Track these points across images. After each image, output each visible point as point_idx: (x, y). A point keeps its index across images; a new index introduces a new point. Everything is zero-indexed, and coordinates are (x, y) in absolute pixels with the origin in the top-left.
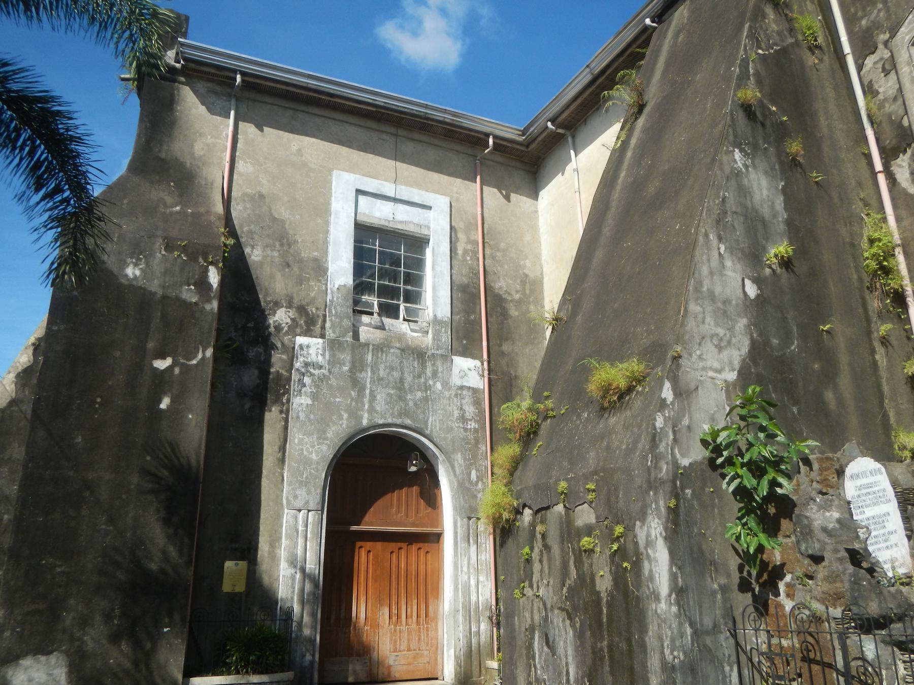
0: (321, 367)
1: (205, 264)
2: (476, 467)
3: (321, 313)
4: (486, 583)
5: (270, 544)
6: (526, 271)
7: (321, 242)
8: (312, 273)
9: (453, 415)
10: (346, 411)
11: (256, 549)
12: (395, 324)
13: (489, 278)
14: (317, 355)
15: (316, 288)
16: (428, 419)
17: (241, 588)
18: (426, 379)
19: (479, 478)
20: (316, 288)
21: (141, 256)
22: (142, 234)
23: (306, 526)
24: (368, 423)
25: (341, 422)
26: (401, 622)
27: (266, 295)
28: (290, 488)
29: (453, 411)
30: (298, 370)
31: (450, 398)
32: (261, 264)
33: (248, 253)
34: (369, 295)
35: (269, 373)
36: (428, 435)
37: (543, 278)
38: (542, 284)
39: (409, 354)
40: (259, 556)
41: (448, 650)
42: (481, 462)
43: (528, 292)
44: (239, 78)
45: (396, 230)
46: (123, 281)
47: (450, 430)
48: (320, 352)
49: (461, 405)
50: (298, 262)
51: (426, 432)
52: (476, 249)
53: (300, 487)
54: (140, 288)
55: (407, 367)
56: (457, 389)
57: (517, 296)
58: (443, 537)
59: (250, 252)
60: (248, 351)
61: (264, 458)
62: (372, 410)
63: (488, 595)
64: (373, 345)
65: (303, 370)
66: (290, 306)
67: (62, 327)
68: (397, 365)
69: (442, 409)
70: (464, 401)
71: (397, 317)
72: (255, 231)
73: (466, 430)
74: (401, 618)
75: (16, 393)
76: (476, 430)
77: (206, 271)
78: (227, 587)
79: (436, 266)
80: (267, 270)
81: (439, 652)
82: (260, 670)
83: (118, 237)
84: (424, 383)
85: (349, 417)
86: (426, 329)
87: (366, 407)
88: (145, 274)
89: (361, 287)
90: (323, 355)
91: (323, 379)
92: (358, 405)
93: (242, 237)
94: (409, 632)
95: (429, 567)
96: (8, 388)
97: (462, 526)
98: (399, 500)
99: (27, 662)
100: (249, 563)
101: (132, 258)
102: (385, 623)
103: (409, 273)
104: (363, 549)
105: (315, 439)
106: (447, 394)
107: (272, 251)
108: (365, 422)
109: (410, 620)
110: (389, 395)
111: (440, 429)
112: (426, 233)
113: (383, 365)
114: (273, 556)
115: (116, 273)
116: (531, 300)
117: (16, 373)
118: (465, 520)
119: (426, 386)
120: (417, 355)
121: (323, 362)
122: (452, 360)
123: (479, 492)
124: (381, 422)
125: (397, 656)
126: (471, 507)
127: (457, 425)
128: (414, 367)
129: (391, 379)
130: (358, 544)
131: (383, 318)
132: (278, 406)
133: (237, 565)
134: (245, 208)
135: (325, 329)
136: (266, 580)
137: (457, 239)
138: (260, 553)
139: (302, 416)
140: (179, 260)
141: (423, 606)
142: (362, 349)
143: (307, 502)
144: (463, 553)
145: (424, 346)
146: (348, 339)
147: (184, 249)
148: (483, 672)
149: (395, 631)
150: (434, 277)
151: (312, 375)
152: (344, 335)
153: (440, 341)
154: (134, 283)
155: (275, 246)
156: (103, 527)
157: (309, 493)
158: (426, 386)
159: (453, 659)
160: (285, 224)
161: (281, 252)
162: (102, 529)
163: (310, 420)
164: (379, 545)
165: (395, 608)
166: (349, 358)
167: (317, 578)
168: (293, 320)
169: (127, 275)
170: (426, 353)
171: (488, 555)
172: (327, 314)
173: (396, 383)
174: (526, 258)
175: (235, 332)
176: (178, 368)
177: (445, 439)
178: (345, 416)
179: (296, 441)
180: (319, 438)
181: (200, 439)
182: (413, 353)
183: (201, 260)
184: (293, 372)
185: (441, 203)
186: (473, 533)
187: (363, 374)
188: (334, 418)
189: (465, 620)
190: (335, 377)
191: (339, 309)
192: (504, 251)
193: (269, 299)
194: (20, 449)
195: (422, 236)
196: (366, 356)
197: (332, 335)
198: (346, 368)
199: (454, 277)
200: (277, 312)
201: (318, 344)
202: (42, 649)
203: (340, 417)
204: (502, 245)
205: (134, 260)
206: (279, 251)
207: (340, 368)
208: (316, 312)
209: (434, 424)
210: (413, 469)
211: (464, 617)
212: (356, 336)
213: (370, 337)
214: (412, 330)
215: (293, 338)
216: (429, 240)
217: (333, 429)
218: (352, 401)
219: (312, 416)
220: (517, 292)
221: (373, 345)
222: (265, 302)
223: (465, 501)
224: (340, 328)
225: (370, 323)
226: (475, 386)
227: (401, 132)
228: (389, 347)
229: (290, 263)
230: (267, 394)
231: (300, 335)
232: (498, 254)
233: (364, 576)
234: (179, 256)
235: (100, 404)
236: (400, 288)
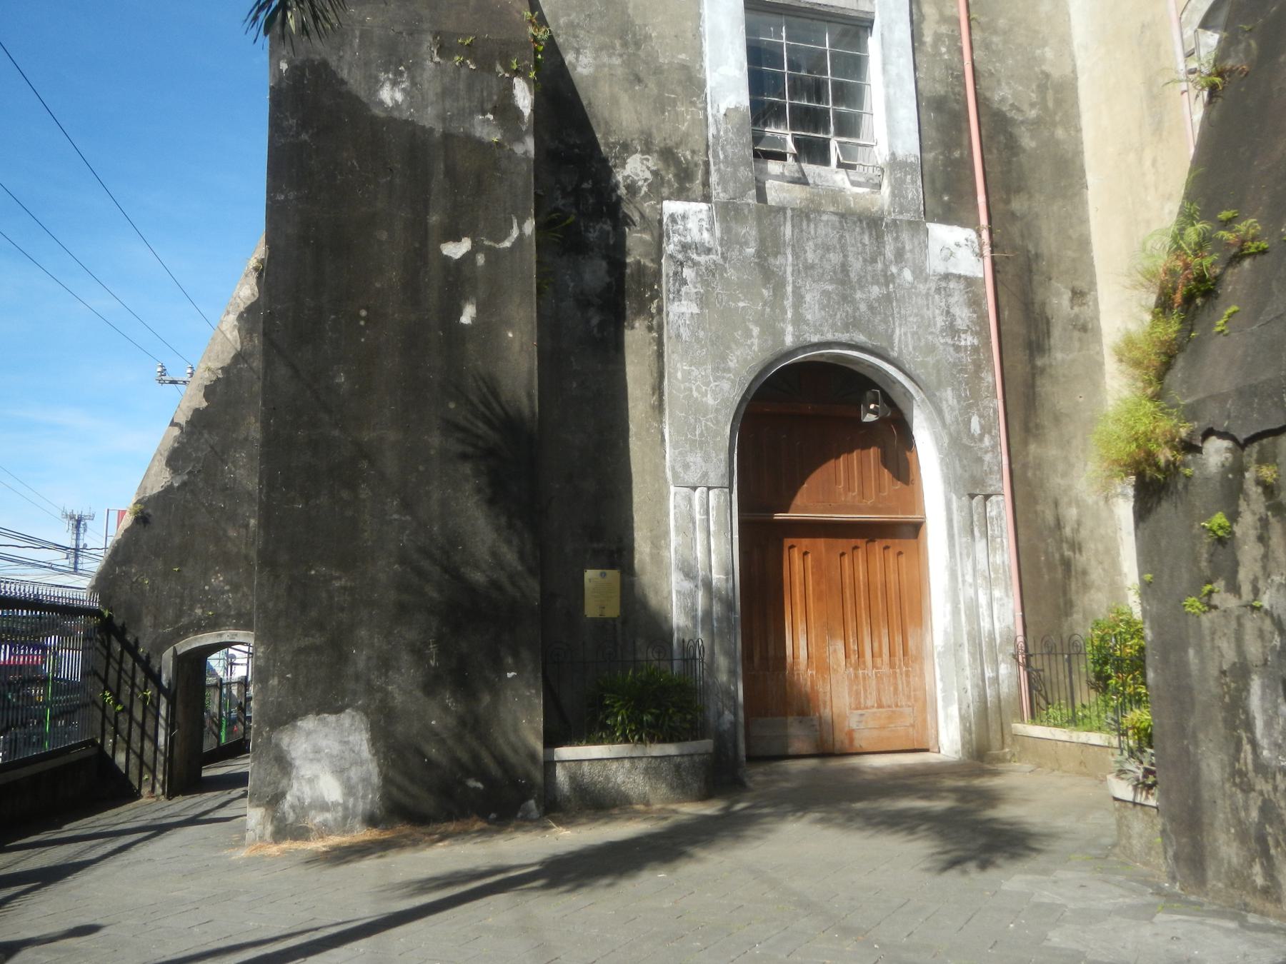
1: (507, 75)
2: (978, 410)
3: (700, 159)
4: (1006, 600)
5: (652, 543)
6: (1045, 68)
7: (689, 35)
8: (679, 89)
9: (935, 325)
10: (756, 323)
11: (630, 550)
12: (823, 174)
13: (984, 83)
14: (700, 231)
15: (688, 117)
16: (893, 332)
17: (613, 611)
18: (884, 264)
19: (986, 429)
20: (688, 117)
21: (402, 68)
22: (398, 28)
23: (707, 513)
24: (793, 342)
25: (749, 342)
26: (864, 663)
27: (607, 133)
28: (677, 451)
29: (934, 318)
30: (671, 256)
31: (927, 295)
32: (595, 79)
33: (570, 62)
34: (777, 126)
35: (623, 265)
36: (894, 359)
37: (1076, 78)
38: (1074, 89)
39: (855, 223)
40: (636, 561)
41: (946, 707)
42: (986, 402)
43: (1051, 104)
45: (815, 7)
46: (377, 112)
47: (931, 349)
48: (705, 226)
49: (948, 307)
50: (655, 73)
51: (891, 353)
52: (956, 33)
53: (691, 451)
54: (406, 121)
55: (853, 246)
56: (939, 279)
57: (1033, 113)
58: (926, 529)
59: (574, 61)
60: (587, 230)
61: (631, 404)
62: (798, 320)
63: (1009, 620)
64: (793, 209)
65: (680, 257)
66: (647, 150)
67: (292, 195)
68: (835, 241)
69: (916, 315)
70: (952, 300)
71: (826, 162)
72: (578, 24)
73: (957, 348)
74: (864, 657)
75: (242, 343)
76: (975, 349)
77: (510, 87)
79: (889, 67)
80: (605, 89)
81: (929, 709)
82: (661, 737)
83: (361, 37)
84: (882, 271)
85: (762, 333)
86: (876, 181)
87: (789, 315)
88: (412, 97)
89: (762, 112)
90: (711, 230)
92: (775, 312)
93: (558, 35)
94: (879, 678)
95: (904, 577)
96: (229, 336)
97: (960, 509)
98: (848, 469)
99: (308, 723)
100: (622, 573)
101: (387, 72)
102: (839, 665)
103: (842, 83)
104: (796, 549)
105: (709, 371)
106: (922, 288)
107: (610, 56)
108: (789, 340)
109: (878, 661)
110: (825, 293)
111: (914, 348)
112: (867, 9)
113: (811, 243)
114: (658, 559)
115: (365, 100)
116: (1057, 118)
117: (238, 313)
118: (965, 499)
119: (885, 276)
120: (868, 224)
121: (712, 243)
122: (927, 231)
123: (986, 452)
124: (815, 339)
125: (862, 715)
126: (973, 478)
127: (942, 341)
128: (864, 245)
129: (828, 267)
130: (788, 542)
131: (803, 165)
132: (645, 319)
133: (603, 575)
135: (709, 187)
136: (653, 601)
137: (922, 17)
138: (637, 557)
139: (685, 333)
140: (463, 71)
141: (898, 639)
142: (775, 217)
143: (705, 475)
144: (965, 552)
145: (876, 209)
146: (750, 201)
147: (469, 51)
148: (1008, 740)
149: (856, 676)
150: (887, 86)
151: (695, 264)
152: (743, 194)
153: (904, 198)
154: (396, 114)
155: (614, 48)
156: (396, 516)
157: (706, 459)
158: (885, 276)
159: (957, 720)
160: (627, 8)
161: (625, 57)
162: (395, 520)
163: (698, 340)
164: (821, 543)
165: (854, 641)
166: (754, 233)
167: (731, 594)
168: (655, 173)
169: (382, 103)
170: (882, 219)
171: (1006, 556)
172: (711, 160)
173: (835, 272)
174: (1045, 43)
175: (562, 198)
176: (483, 255)
177: (924, 364)
178: (756, 331)
179: (679, 375)
180: (716, 369)
181: (530, 372)
182: (861, 221)
183: (499, 68)
184: (663, 261)
186: (978, 521)
187: (780, 260)
188: (738, 334)
189: (975, 660)
190: (735, 268)
191: (729, 149)
192: (1005, 33)
193: (612, 140)
195: (861, 15)
196: (782, 228)
197: (721, 195)
198: (750, 251)
199: (921, 84)
200: (628, 161)
201: (701, 211)
202: (329, 705)
203: (748, 334)
204: (1002, 23)
205: (391, 76)
206: (621, 56)
207: (740, 252)
208: (692, 157)
209: (903, 339)
210: (870, 418)
211: (973, 655)
212: (761, 195)
213: (784, 198)
214: (854, 183)
215: (658, 203)
216: (872, 22)
217: (738, 353)
218: (764, 305)
219: (701, 334)
220: (1032, 105)
221: (793, 209)
222: (607, 144)
223: (963, 467)
224: (735, 182)
225: (783, 174)
226: (969, 274)
228: (819, 212)
229: (642, 75)
230: (623, 299)
231: (669, 199)
232: (995, 39)
233: (800, 592)
234: (463, 63)
235: (367, 319)
236: (827, 111)
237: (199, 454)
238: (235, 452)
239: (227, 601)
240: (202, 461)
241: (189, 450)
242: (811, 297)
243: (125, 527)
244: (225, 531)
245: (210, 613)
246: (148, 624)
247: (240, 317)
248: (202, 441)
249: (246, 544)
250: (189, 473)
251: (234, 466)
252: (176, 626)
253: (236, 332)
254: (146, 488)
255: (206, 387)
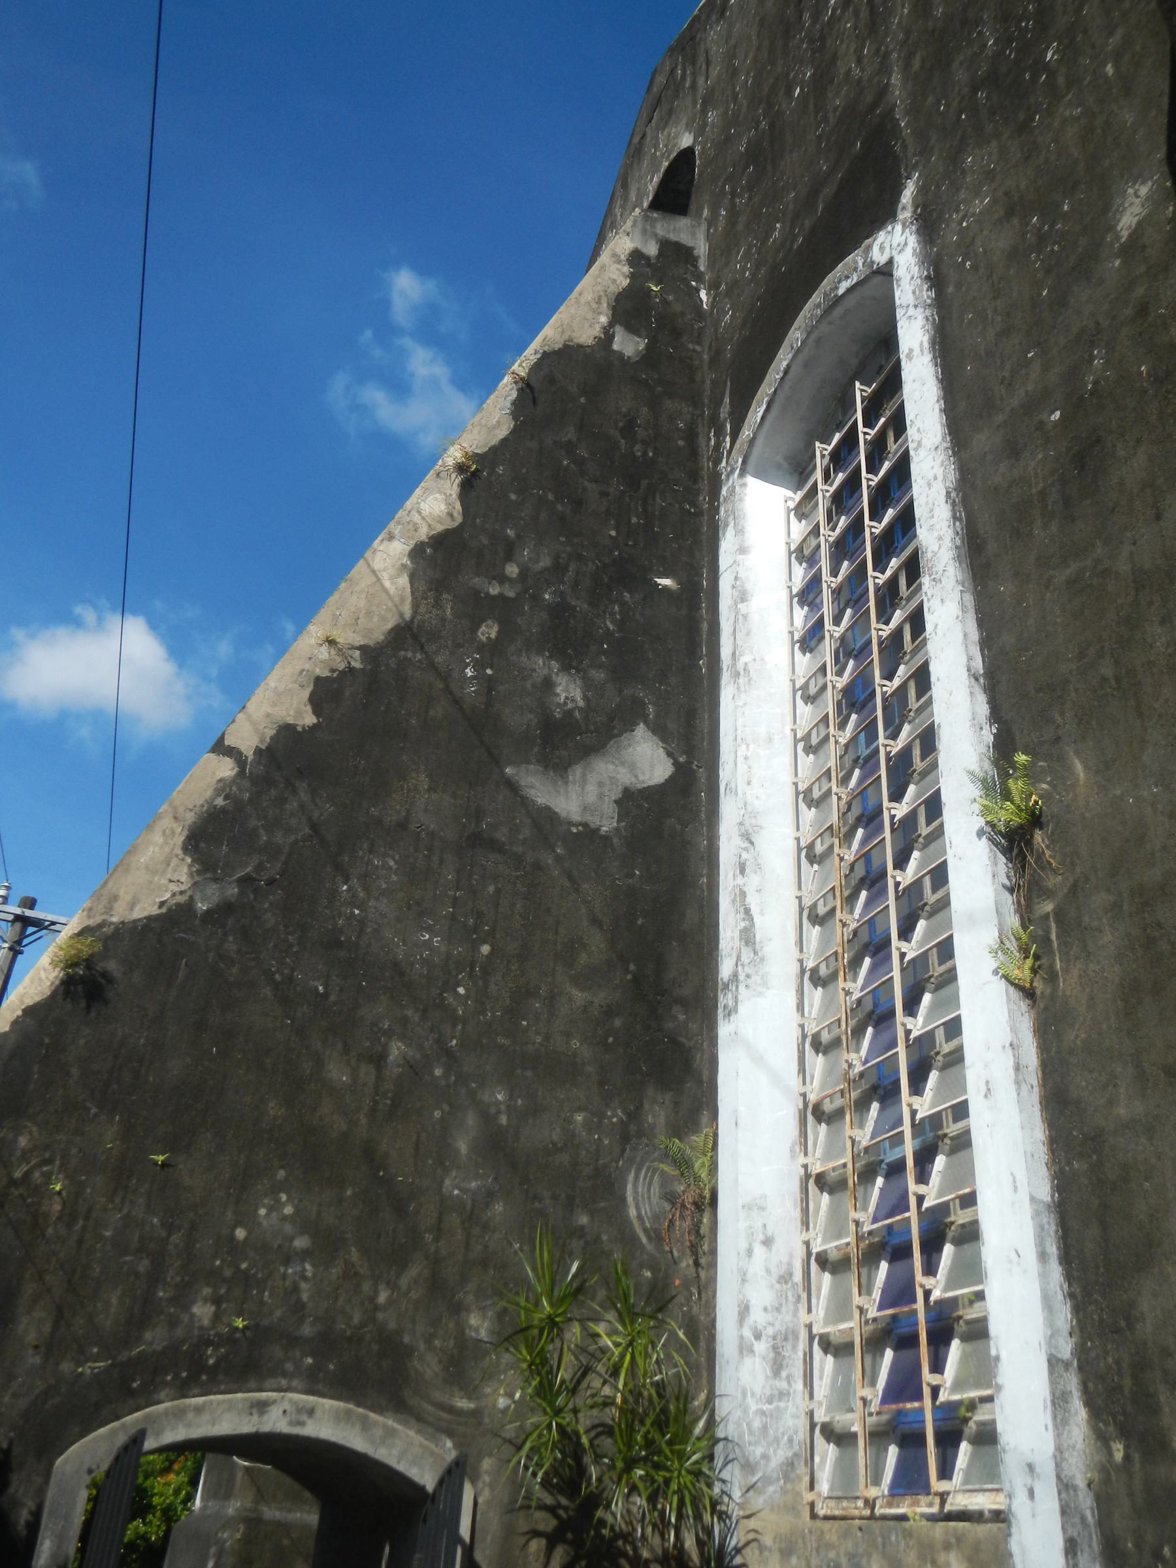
75: (415, 606)
96: (387, 584)
117: (412, 543)
194: (434, 796)
237: (279, 838)
238: (371, 852)
239: (296, 1289)
240: (283, 858)
241: (253, 823)
243: (29, 1002)
244: (319, 1063)
245: (239, 1323)
246: (32, 1337)
247: (417, 552)
248: (292, 805)
249: (373, 1111)
250: (245, 881)
251: (366, 889)
252: (123, 1356)
253: (404, 581)
254: (115, 898)
255: (318, 680)
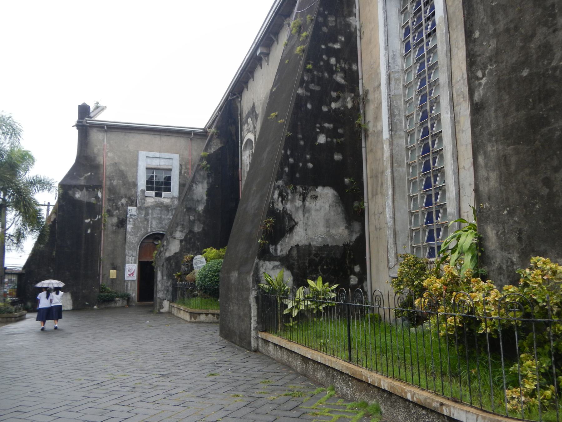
0: (135, 216)
17: (115, 277)
44: (105, 126)
62: (151, 227)
66: (126, 197)
78: (111, 277)
87: (149, 226)
90: (136, 212)
91: (137, 219)
134: (111, 168)
151: (133, 218)
178: (143, 229)
185: (176, 157)
188: (140, 230)
198: (143, 215)
203: (141, 230)
227: (161, 134)
242: (154, 223)
